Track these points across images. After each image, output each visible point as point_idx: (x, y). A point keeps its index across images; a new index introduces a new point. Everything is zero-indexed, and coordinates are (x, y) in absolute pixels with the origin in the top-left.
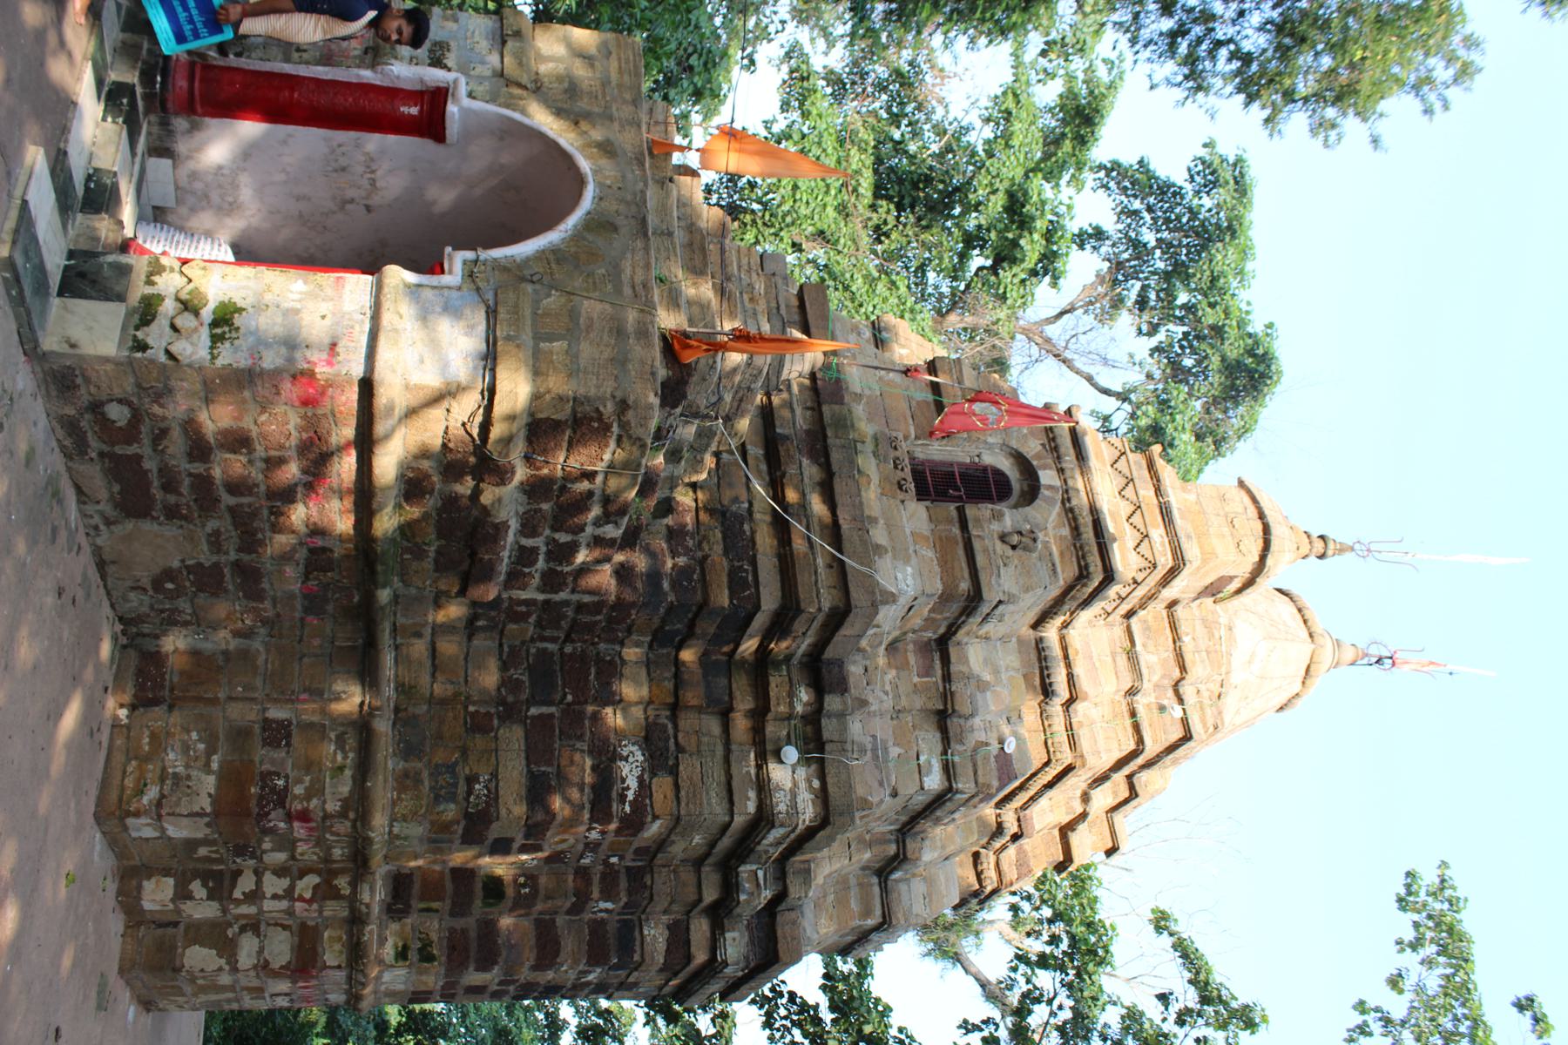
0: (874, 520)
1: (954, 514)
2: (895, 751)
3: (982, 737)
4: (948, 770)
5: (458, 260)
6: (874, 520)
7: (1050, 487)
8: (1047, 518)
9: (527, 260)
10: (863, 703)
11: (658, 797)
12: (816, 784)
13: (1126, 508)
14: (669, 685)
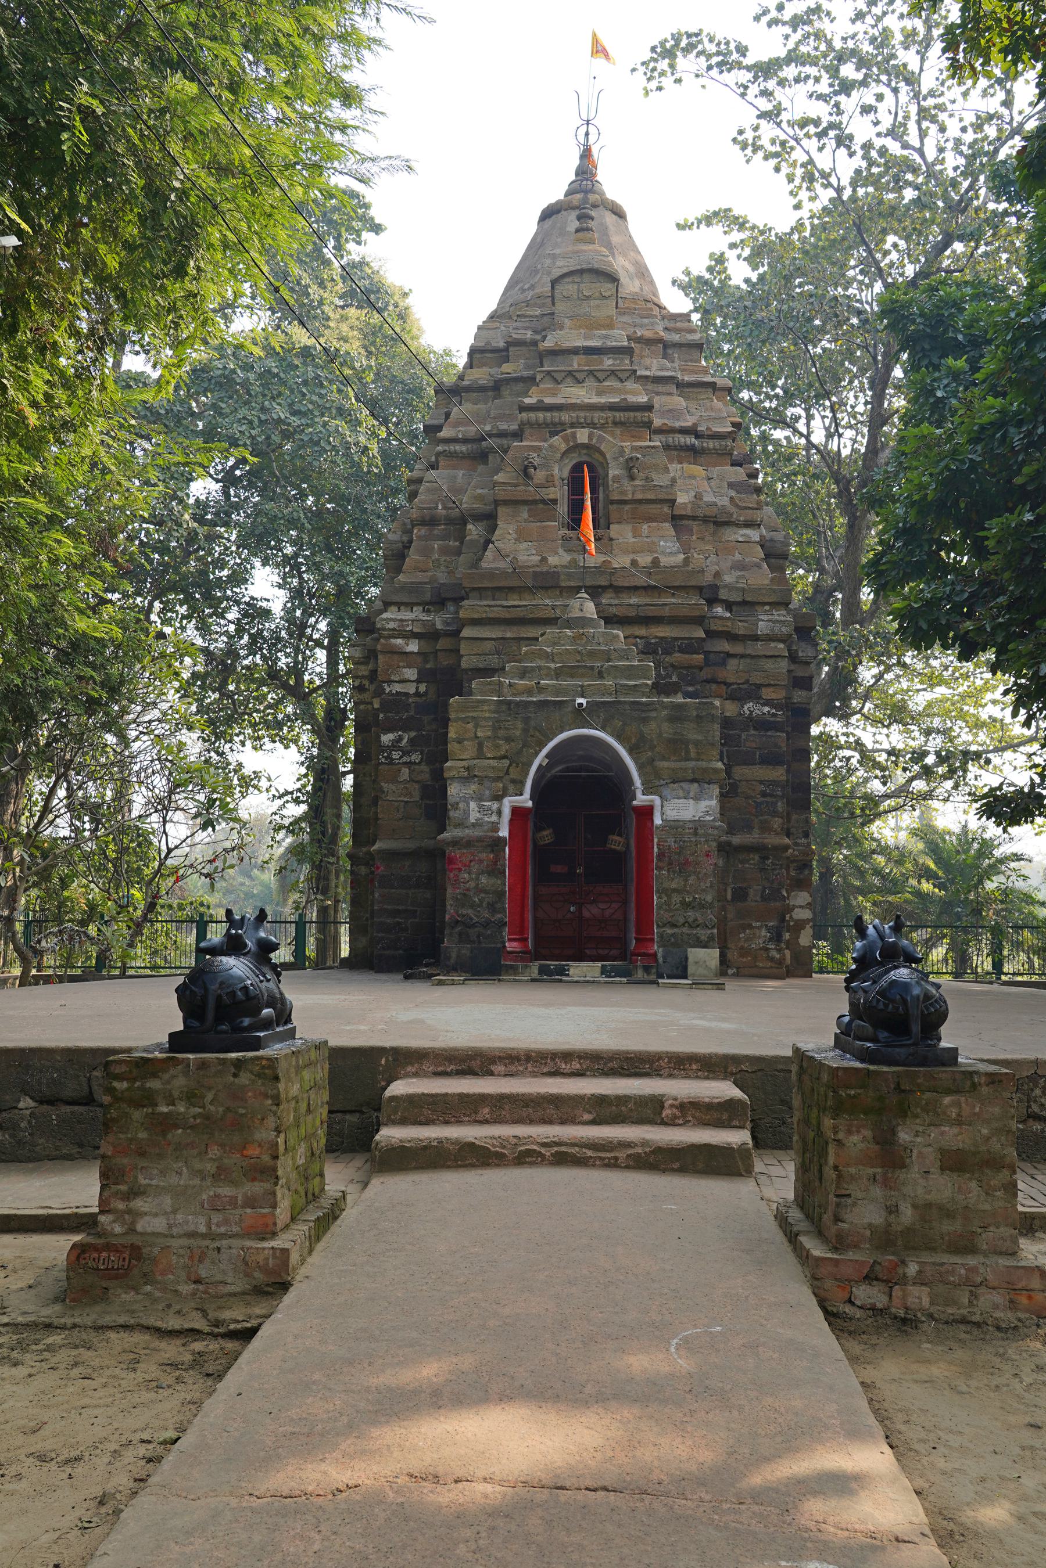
0: (634, 563)
1: (615, 506)
2: (738, 557)
3: (725, 501)
4: (750, 524)
5: (641, 799)
6: (634, 563)
7: (591, 436)
8: (616, 446)
9: (636, 763)
10: (717, 575)
11: (774, 696)
12: (767, 608)
13: (590, 382)
14: (714, 686)
